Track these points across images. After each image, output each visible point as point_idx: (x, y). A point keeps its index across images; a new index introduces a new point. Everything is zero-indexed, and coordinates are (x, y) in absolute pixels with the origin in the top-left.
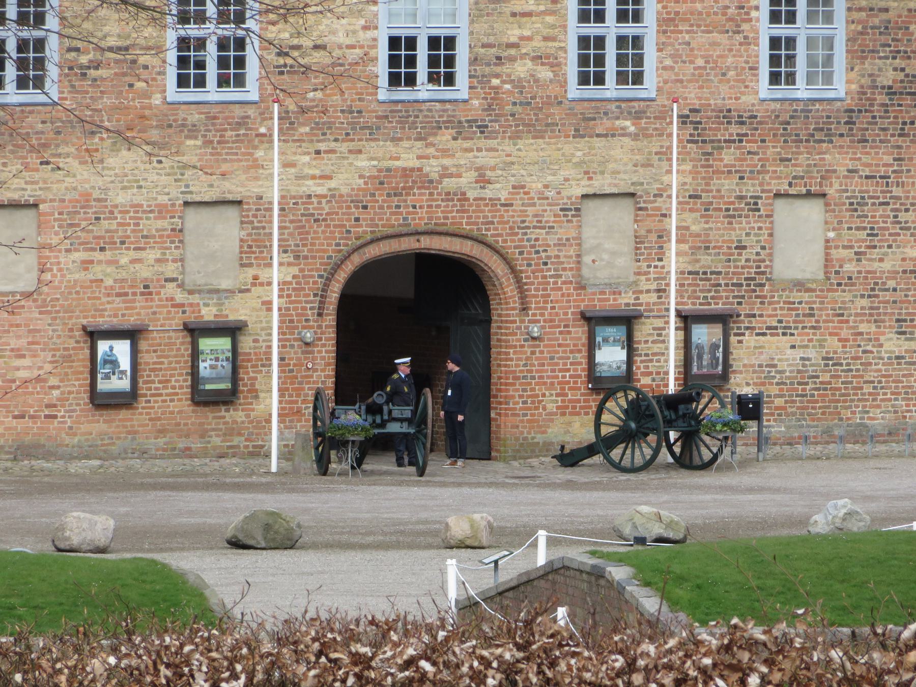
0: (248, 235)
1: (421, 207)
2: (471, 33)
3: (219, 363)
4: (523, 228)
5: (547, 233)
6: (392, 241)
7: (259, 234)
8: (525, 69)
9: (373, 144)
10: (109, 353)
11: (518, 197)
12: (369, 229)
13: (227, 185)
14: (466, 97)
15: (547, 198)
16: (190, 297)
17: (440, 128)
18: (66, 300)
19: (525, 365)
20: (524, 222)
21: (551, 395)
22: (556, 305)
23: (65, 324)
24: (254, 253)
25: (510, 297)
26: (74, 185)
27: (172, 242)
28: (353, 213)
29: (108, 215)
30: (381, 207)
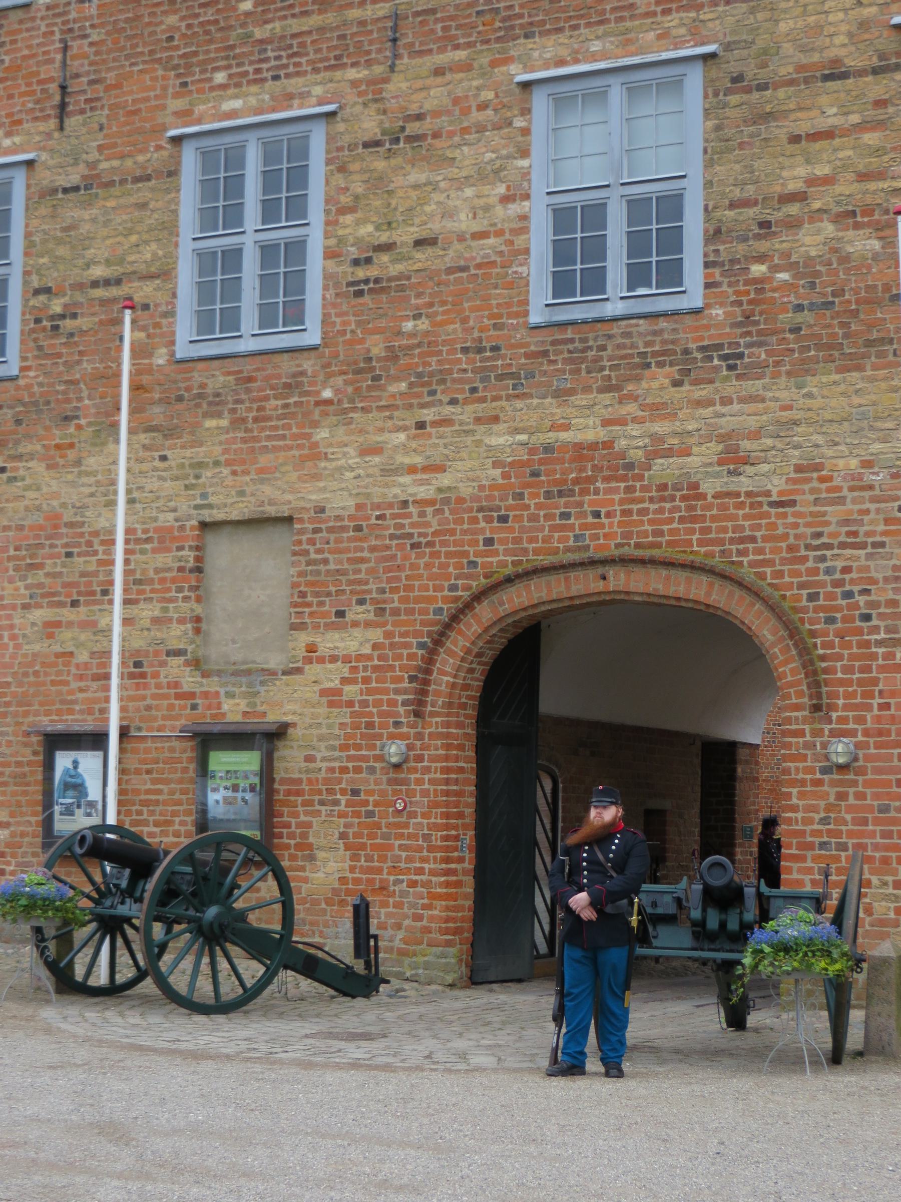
0: (301, 574)
1: (608, 515)
2: (708, 184)
3: (239, 795)
4: (817, 548)
5: (869, 556)
6: (552, 578)
7: (318, 573)
8: (820, 238)
9: (519, 404)
10: (73, 773)
11: (806, 487)
12: (510, 559)
13: (268, 491)
14: (699, 303)
15: (871, 487)
16: (204, 681)
17: (648, 366)
18: (20, 684)
19: (824, 821)
20: (819, 535)
21: (885, 884)
22: (892, 701)
23: (18, 724)
24: (309, 605)
25: (791, 685)
26: (37, 503)
27: (180, 590)
28: (483, 530)
29: (84, 548)
30: (534, 518)
